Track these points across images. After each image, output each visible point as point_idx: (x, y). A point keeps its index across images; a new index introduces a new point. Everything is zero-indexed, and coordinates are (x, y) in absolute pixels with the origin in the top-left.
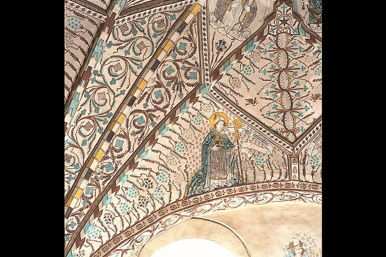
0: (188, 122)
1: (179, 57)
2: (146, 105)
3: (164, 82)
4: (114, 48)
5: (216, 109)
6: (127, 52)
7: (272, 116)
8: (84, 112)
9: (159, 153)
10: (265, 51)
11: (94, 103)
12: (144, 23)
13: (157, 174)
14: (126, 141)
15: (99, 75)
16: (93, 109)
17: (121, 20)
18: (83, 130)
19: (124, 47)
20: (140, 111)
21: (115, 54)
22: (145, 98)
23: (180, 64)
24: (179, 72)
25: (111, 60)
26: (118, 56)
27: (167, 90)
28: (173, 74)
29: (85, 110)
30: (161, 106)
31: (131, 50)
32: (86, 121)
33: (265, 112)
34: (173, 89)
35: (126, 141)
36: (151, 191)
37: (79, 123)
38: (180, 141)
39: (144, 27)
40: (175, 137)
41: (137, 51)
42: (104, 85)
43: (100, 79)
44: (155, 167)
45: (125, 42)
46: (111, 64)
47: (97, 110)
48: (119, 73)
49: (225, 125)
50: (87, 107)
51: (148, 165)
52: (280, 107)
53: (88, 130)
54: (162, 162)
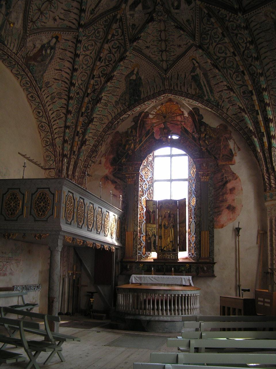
0: (261, 32)
1: (227, 18)
2: (243, 47)
3: (236, 32)
4: (211, 46)
5: (261, 14)
6: (215, 41)
8: (230, 74)
9: (267, 57)
12: (205, 28)
13: (274, 66)
15: (219, 59)
16: (232, 69)
17: (196, 42)
18: (238, 79)
19: (212, 42)
20: (244, 51)
21: (214, 47)
22: (239, 45)
23: (231, 19)
24: (235, 22)
25: (215, 50)
26: (215, 46)
27: (240, 34)
28: (235, 25)
29: (230, 73)
30: (245, 41)
31: (216, 39)
32: (235, 75)
34: (241, 30)
37: (234, 79)
39: (207, 29)
41: (217, 36)
42: (225, 58)
43: (221, 59)
45: (210, 41)
46: (217, 51)
48: (223, 49)
50: (229, 71)
53: (239, 77)
54: (271, 60)
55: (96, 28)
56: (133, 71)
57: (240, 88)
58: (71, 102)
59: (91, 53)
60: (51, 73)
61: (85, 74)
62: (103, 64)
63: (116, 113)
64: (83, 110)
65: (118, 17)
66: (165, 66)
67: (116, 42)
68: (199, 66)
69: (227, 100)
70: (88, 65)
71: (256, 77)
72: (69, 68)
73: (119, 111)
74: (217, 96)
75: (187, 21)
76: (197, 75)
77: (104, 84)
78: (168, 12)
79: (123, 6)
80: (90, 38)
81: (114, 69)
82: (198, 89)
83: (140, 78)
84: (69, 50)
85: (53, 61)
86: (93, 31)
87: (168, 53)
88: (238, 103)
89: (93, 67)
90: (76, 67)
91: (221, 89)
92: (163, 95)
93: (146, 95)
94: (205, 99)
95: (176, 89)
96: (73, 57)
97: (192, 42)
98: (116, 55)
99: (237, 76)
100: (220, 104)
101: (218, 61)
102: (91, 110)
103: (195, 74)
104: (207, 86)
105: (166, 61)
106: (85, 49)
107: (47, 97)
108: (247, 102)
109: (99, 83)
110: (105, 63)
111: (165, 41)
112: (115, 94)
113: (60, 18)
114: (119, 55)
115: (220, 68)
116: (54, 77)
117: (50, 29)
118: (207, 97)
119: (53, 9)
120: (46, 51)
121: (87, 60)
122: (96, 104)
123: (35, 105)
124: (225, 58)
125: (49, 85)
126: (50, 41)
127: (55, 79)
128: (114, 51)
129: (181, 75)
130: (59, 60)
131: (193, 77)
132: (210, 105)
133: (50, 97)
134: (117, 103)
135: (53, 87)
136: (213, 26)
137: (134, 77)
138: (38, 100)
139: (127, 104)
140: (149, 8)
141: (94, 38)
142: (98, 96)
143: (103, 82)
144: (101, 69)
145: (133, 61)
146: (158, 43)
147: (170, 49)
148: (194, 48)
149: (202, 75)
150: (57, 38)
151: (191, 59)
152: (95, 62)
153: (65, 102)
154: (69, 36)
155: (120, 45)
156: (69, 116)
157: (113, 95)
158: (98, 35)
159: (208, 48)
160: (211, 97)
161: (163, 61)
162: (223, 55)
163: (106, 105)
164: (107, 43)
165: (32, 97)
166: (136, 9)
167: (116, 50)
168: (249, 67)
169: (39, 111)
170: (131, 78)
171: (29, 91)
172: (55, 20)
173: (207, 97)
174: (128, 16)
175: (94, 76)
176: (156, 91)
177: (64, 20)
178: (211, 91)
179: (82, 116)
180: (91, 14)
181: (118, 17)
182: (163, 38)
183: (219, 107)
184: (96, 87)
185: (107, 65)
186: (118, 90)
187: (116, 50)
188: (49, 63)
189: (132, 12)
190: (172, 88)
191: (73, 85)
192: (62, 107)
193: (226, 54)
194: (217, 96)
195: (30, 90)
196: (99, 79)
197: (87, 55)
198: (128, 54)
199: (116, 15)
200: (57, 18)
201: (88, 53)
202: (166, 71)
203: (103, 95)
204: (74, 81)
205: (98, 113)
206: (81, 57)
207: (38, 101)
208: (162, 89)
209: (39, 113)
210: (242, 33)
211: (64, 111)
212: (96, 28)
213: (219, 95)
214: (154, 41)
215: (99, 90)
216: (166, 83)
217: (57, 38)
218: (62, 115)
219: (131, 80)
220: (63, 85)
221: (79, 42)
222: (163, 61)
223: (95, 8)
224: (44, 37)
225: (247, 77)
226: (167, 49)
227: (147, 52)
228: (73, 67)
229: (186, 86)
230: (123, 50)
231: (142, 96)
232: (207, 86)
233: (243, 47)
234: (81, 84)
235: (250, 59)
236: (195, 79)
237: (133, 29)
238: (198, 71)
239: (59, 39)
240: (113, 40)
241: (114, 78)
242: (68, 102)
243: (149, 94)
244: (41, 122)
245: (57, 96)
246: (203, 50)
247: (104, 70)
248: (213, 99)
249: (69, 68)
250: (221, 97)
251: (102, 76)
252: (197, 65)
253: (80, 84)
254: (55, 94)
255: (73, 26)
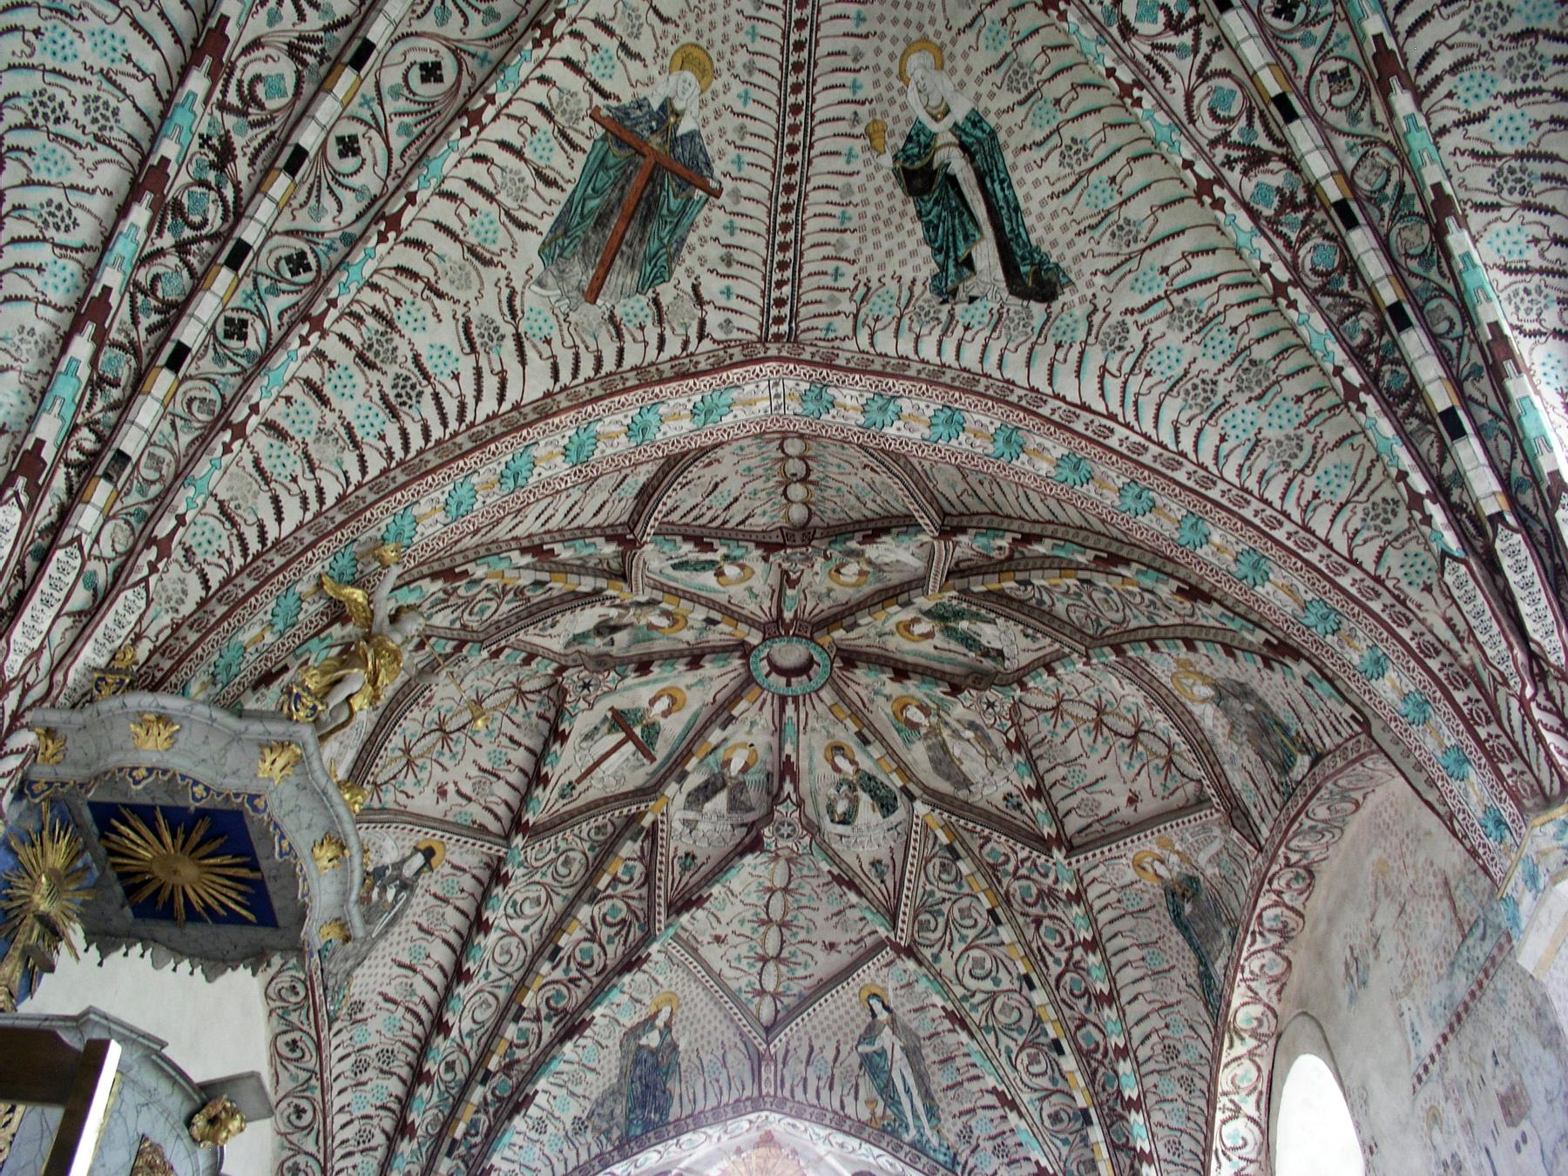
2: (1057, 962)
4: (945, 954)
7: (1172, 785)
8: (1008, 1051)
10: (1054, 733)
11: (1008, 1027)
12: (932, 894)
14: (1090, 1027)
18: (1035, 1069)
23: (1023, 871)
27: (1051, 917)
28: (1034, 891)
30: (1069, 942)
32: (1023, 1055)
33: (1159, 790)
35: (1090, 1027)
36: (1183, 1058)
38: (1144, 952)
39: (939, 895)
40: (1134, 954)
41: (969, 922)
42: (992, 997)
43: (979, 997)
44: (1155, 1021)
47: (1020, 1031)
48: (988, 964)
49: (1162, 862)
50: (1005, 1041)
51: (1145, 1027)
52: (1161, 763)
55: (563, 846)
56: (655, 1016)
57: (1042, 1099)
58: (423, 1091)
59: (526, 929)
60: (380, 970)
61: (491, 1000)
62: (558, 974)
63: (572, 1164)
64: (459, 1133)
65: (647, 822)
66: (766, 1013)
67: (620, 904)
68: (893, 1022)
69: (989, 1145)
70: (508, 969)
71: (1101, 1063)
72: (441, 968)
73: (584, 1157)
74: (951, 1128)
75: (873, 864)
76: (882, 1053)
77: (551, 1045)
78: (813, 829)
79: (671, 789)
80: (537, 878)
81: (595, 996)
82: (881, 1104)
83: (674, 1047)
84: (460, 904)
85: (396, 929)
86: (553, 855)
87: (783, 969)
88: (1036, 1155)
89: (523, 979)
90: (470, 965)
91: (967, 1106)
92: (752, 1116)
93: (687, 1111)
94: (907, 1138)
95: (799, 1095)
96: (465, 932)
97: (882, 932)
98: (610, 949)
99: (1033, 1060)
100: (961, 1159)
101: (967, 1006)
102: (487, 1135)
103: (877, 1046)
104: (915, 1092)
105: (775, 996)
106: (510, 911)
107: (341, 1059)
108: (1065, 1150)
109: (532, 1039)
110: (567, 971)
111: (783, 925)
112: (579, 1090)
113: (459, 792)
114: (621, 949)
115: (974, 1028)
116: (385, 989)
117: (420, 820)
118: (913, 1132)
119: (445, 760)
120: (383, 889)
121: (508, 952)
122: (510, 1118)
123: (294, 1078)
124: (992, 997)
125: (359, 1016)
126: (404, 861)
127: (387, 999)
128: (605, 932)
129: (822, 1049)
130: (415, 933)
131: (866, 1060)
132: (924, 1159)
133: (352, 1059)
134: (580, 1125)
135: (373, 1025)
136: (960, 886)
137: (652, 1039)
138: (311, 1062)
139: (616, 1133)
140: (751, 809)
141: (548, 880)
142: (518, 1088)
143: (546, 1039)
144: (549, 991)
145: (660, 979)
146: (755, 930)
147: (793, 954)
148: (888, 954)
149: (898, 1053)
150: (429, 853)
151: (865, 994)
152: (533, 962)
153: (397, 1088)
154: (469, 856)
155: (629, 917)
156: (405, 1147)
157: (572, 1094)
158: (563, 871)
159: (936, 958)
160: (928, 1132)
161: (762, 992)
162: (988, 985)
163: (540, 1127)
164: (593, 900)
165: (293, 1045)
166: (708, 806)
167: (613, 931)
168: (1078, 1028)
169: (304, 1104)
170: (643, 1041)
171: (289, 1023)
172: (442, 793)
173: (913, 1132)
174: (677, 825)
175: (522, 1009)
176: (725, 1099)
177: (469, 799)
178: (932, 1112)
179: (449, 1154)
180: (563, 796)
181: (647, 822)
182: (776, 914)
183: (959, 1170)
184: (520, 1054)
185: (572, 981)
186: (591, 1077)
187: (613, 931)
188: (383, 934)
189: (691, 815)
190: (787, 1093)
191: (441, 1027)
192: (383, 1107)
193: (997, 982)
194: (951, 1128)
195: (294, 1017)
196: (533, 1026)
197: (513, 934)
198: (654, 948)
199: (642, 815)
200: (451, 788)
201: (517, 925)
202: (768, 1030)
203: (542, 1084)
204: (449, 1017)
205: (508, 1153)
206: (494, 935)
207: (311, 1065)
208: (747, 1093)
209: (300, 1112)
210: (1059, 914)
211: (388, 1124)
212: (563, 846)
213: (959, 1126)
214: (742, 922)
215: (525, 1067)
216: (767, 1073)
217: (429, 853)
218: (379, 1139)
219: (640, 1047)
220: (407, 1026)
221: (504, 880)
222: (762, 992)
223: (579, 781)
224: (389, 843)
225: (1069, 1063)
226: (785, 954)
227: (711, 953)
228: (458, 964)
229: (837, 1088)
230: (639, 934)
231: (674, 1112)
232: (915, 1092)
233: (1057, 962)
234: (470, 1034)
235: (1083, 1002)
236: (873, 1065)
237: (685, 868)
238: (886, 1038)
239: (434, 861)
240: (610, 897)
241: (588, 1032)
242: (410, 1093)
243: (700, 1106)
244: (298, 1151)
245: (376, 1063)
246: (920, 963)
247: (559, 994)
248: (935, 1141)
249: (441, 968)
250: (966, 1134)
251: (548, 1018)
252: (883, 1016)
253: (465, 1030)
254: (372, 1053)
255: (493, 826)
